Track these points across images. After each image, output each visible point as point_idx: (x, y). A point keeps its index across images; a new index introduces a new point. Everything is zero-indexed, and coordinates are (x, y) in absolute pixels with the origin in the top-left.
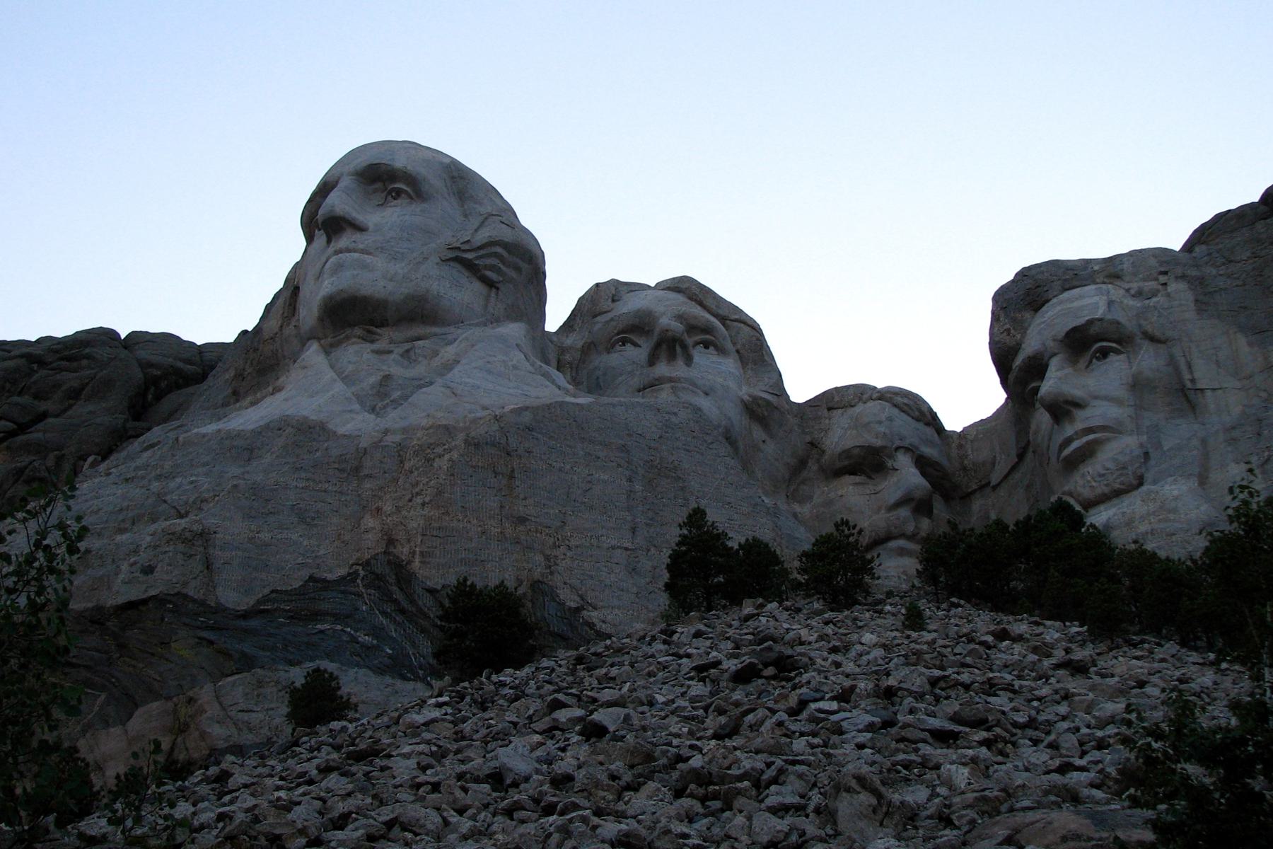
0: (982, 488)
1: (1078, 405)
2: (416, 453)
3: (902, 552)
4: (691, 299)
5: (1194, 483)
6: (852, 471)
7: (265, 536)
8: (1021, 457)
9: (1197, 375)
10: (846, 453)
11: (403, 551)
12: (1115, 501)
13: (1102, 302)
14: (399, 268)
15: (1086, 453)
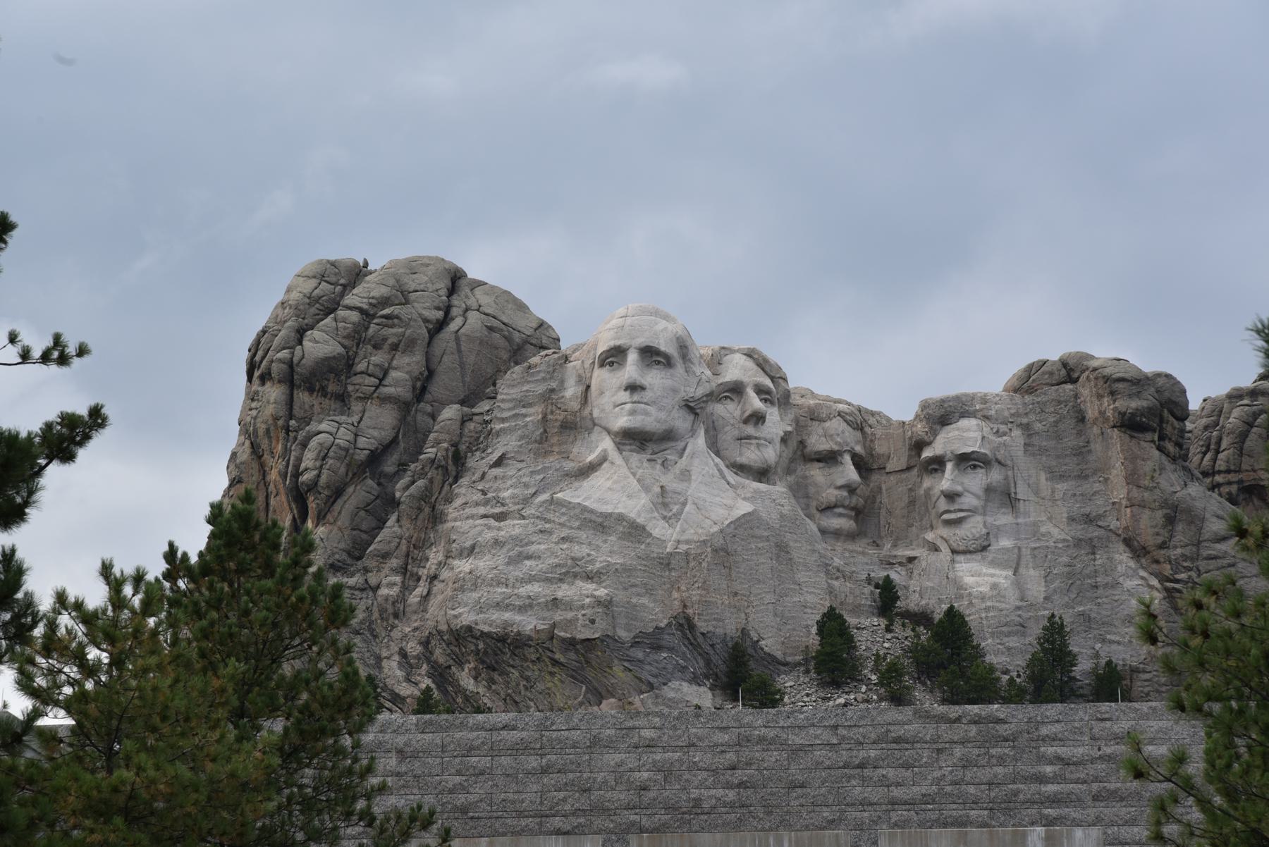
0: (880, 469)
1: (958, 495)
2: (694, 559)
3: (840, 515)
4: (759, 365)
5: (1010, 573)
6: (819, 461)
7: (634, 600)
8: (909, 468)
9: (1018, 490)
10: (816, 453)
11: (690, 611)
12: (968, 556)
13: (978, 435)
14: (662, 415)
15: (957, 522)
